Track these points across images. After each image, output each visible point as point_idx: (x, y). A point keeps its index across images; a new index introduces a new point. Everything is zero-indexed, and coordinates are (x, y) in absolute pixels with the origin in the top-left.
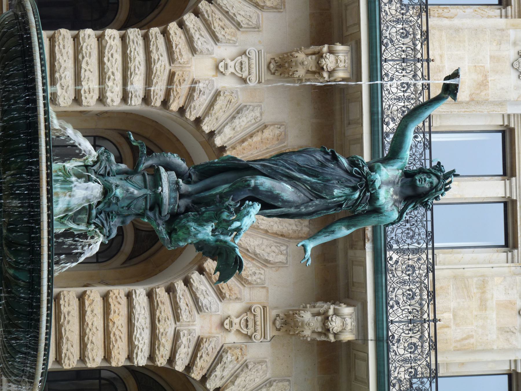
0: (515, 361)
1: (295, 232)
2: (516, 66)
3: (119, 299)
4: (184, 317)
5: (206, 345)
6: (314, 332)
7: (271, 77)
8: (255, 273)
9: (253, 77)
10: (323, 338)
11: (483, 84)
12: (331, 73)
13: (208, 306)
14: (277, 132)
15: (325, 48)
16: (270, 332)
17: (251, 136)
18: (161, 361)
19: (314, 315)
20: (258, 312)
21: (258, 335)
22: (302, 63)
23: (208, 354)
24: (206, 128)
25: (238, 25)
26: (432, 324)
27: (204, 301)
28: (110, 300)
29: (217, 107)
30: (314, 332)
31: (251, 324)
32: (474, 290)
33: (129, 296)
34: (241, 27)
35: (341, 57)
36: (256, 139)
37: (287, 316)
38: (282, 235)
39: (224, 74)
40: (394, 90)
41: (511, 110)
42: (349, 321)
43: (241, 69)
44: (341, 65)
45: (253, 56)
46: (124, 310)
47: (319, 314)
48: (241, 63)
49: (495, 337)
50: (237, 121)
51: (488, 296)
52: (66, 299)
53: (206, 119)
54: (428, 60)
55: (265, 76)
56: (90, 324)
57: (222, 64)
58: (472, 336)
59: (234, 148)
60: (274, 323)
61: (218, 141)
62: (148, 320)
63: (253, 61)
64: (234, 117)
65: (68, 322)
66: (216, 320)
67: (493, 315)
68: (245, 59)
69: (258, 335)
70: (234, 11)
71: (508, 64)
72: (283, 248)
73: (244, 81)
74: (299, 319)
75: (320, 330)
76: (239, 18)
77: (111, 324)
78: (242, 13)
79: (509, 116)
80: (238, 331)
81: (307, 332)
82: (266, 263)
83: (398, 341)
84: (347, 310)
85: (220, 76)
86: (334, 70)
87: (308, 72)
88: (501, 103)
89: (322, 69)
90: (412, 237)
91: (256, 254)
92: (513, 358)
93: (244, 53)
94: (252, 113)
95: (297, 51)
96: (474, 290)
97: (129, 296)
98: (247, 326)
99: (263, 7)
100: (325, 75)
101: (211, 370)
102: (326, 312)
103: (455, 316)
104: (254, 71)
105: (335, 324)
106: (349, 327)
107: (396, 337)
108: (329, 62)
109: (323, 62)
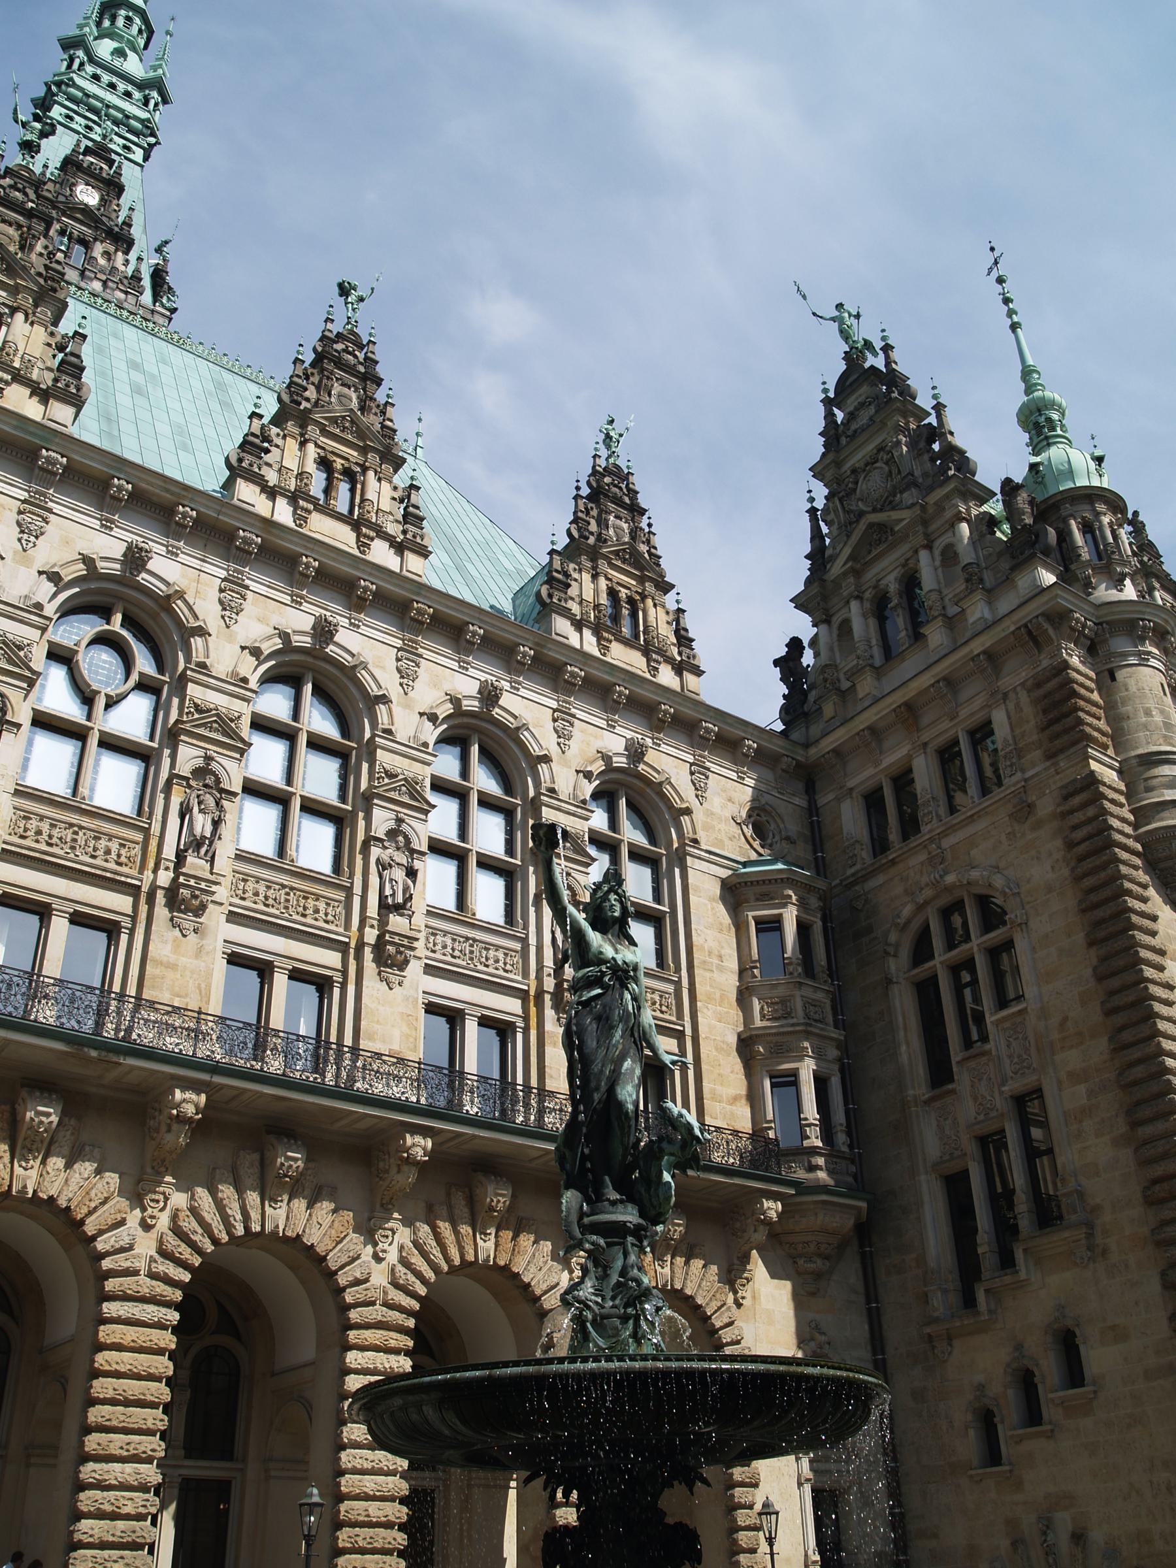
1: (72, 1134)
5: (169, 1245)
13: (131, 1237)
18: (178, 1295)
19: (169, 1130)
23: (179, 1246)
27: (125, 1241)
32: (157, 972)
49: (203, 964)
51: (165, 959)
52: (100, 1390)
56: (129, 1367)
58: (199, 984)
65: (124, 1391)
67: (183, 960)
83: (213, 1052)
96: (157, 972)
98: (158, 1201)
101: (192, 1245)
103: (178, 996)
107: (209, 1053)
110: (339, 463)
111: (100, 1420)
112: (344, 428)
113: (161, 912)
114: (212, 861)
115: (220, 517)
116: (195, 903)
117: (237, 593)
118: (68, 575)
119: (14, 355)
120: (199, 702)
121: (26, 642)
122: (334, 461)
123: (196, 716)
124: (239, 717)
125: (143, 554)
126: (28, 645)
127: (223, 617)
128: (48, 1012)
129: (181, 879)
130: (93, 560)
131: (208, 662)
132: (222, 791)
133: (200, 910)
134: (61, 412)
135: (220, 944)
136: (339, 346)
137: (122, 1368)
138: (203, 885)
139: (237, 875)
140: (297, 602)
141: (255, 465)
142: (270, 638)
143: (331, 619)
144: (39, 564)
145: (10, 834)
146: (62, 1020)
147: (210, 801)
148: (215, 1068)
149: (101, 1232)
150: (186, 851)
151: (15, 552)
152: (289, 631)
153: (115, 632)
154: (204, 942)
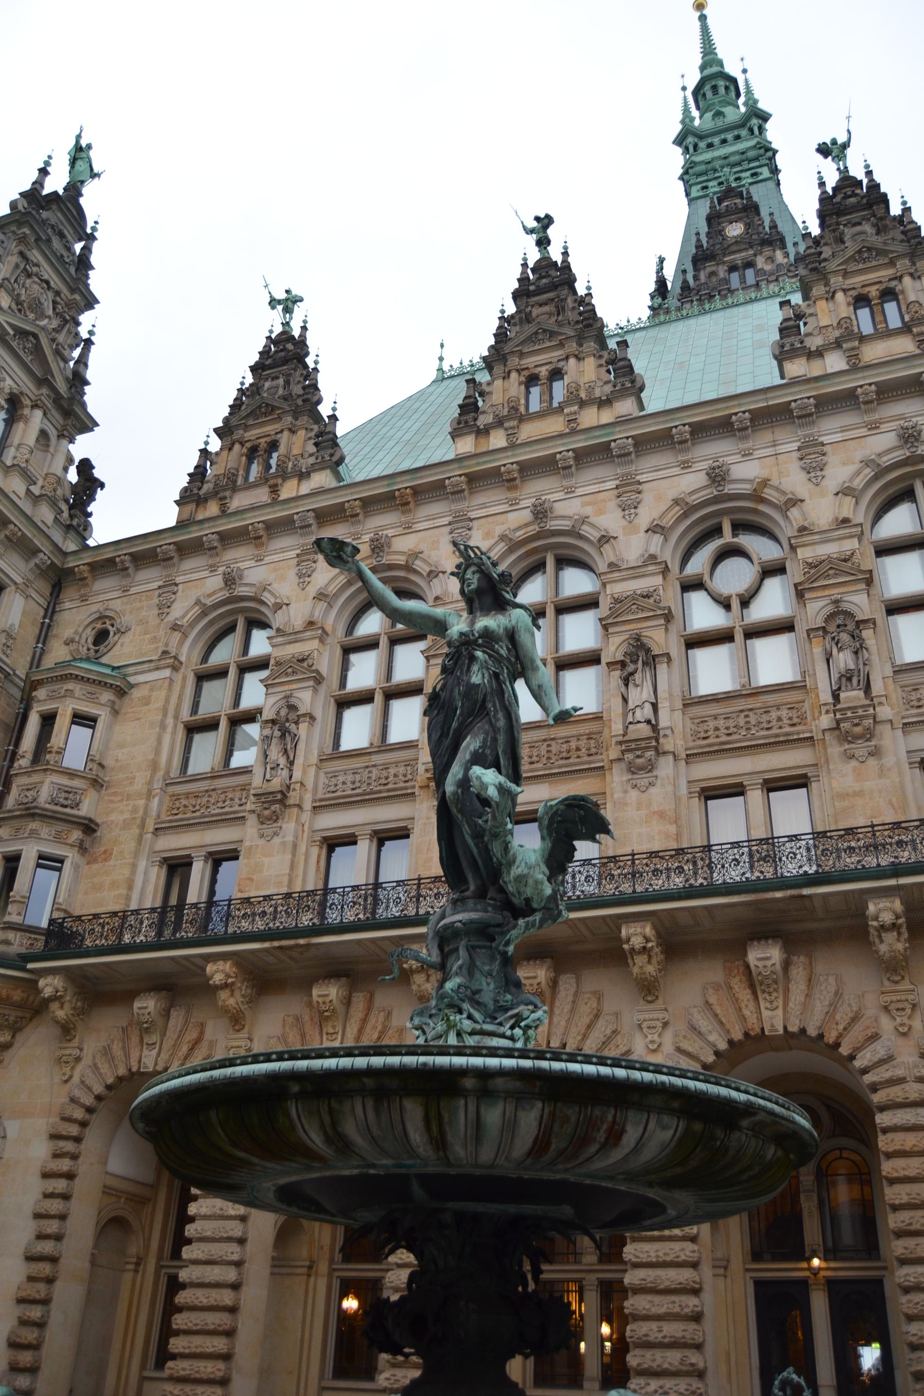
0: (910, 763)
2: (644, 789)
3: (889, 1141)
4: (900, 1072)
6: (898, 940)
7: (660, 1000)
8: (850, 1005)
9: (661, 1016)
10: (904, 930)
11: (661, 815)
12: (647, 940)
14: (711, 991)
15: (626, 946)
16: (906, 985)
17: (716, 1015)
19: (882, 941)
20: (886, 998)
21: (910, 997)
22: (641, 967)
24: (711, 1058)
25: (614, 1032)
26: (876, 828)
28: (890, 1150)
29: (690, 1049)
30: (898, 940)
31: (900, 1005)
33: (885, 1131)
34: (617, 1029)
35: (631, 931)
36: (718, 1010)
37: (887, 970)
38: (810, 981)
39: (660, 1044)
40: (660, 882)
41: (683, 790)
42: (881, 905)
43: (654, 1027)
44: (639, 930)
45: (641, 1017)
46: (900, 1136)
47: (880, 937)
48: (649, 1028)
50: (703, 1030)
52: (893, 1197)
53: (702, 1058)
54: (633, 855)
55: (659, 1004)
56: (917, 1171)
57: (651, 1046)
59: (728, 1031)
60: (896, 982)
61: (723, 1046)
62: (908, 1110)
63: (647, 1016)
64: (700, 1033)
65: (918, 1194)
66: (901, 1041)
68: (644, 1025)
69: (910, 997)
70: (601, 1036)
71: (643, 795)
72: (822, 978)
73: (665, 1025)
74: (887, 955)
75: (895, 934)
76: (608, 1032)
77: (916, 1149)
78: (603, 1029)
79: (690, 793)
80: (910, 1017)
81: (900, 946)
82: (838, 994)
83: (896, 857)
84: (872, 908)
85: (663, 1048)
86: (645, 937)
87: (649, 962)
88: (677, 799)
89: (644, 948)
90: (795, 854)
91: (830, 1005)
92: (907, 765)
93: (640, 1026)
94: (695, 1015)
95: (632, 974)
97: (885, 1131)
98: (903, 1009)
99: (598, 1010)
100: (650, 945)
102: (876, 928)
104: (655, 1016)
105: (887, 918)
106: (888, 904)
107: (892, 860)
108: (637, 942)
109: (637, 947)
110: (873, 292)
111: (901, 1225)
112: (864, 259)
113: (835, 749)
114: (868, 689)
115: (771, 403)
116: (858, 730)
117: (814, 453)
118: (667, 522)
119: (577, 391)
120: (810, 560)
121: (651, 589)
122: (869, 292)
123: (812, 571)
124: (853, 554)
125: (717, 471)
126: (655, 591)
127: (810, 480)
128: (733, 873)
129: (838, 716)
130: (683, 499)
131: (806, 524)
132: (858, 623)
133: (869, 735)
134: (626, 407)
135: (903, 755)
136: (838, 199)
137: (911, 1173)
138: (860, 712)
139: (906, 689)
140: (874, 427)
141: (796, 343)
142: (858, 473)
143: (906, 424)
144: (644, 527)
145: (694, 741)
146: (747, 875)
147: (845, 637)
148: (897, 870)
149: (858, 1049)
150: (839, 689)
151: (624, 528)
152: (873, 457)
153: (727, 543)
154: (884, 761)
